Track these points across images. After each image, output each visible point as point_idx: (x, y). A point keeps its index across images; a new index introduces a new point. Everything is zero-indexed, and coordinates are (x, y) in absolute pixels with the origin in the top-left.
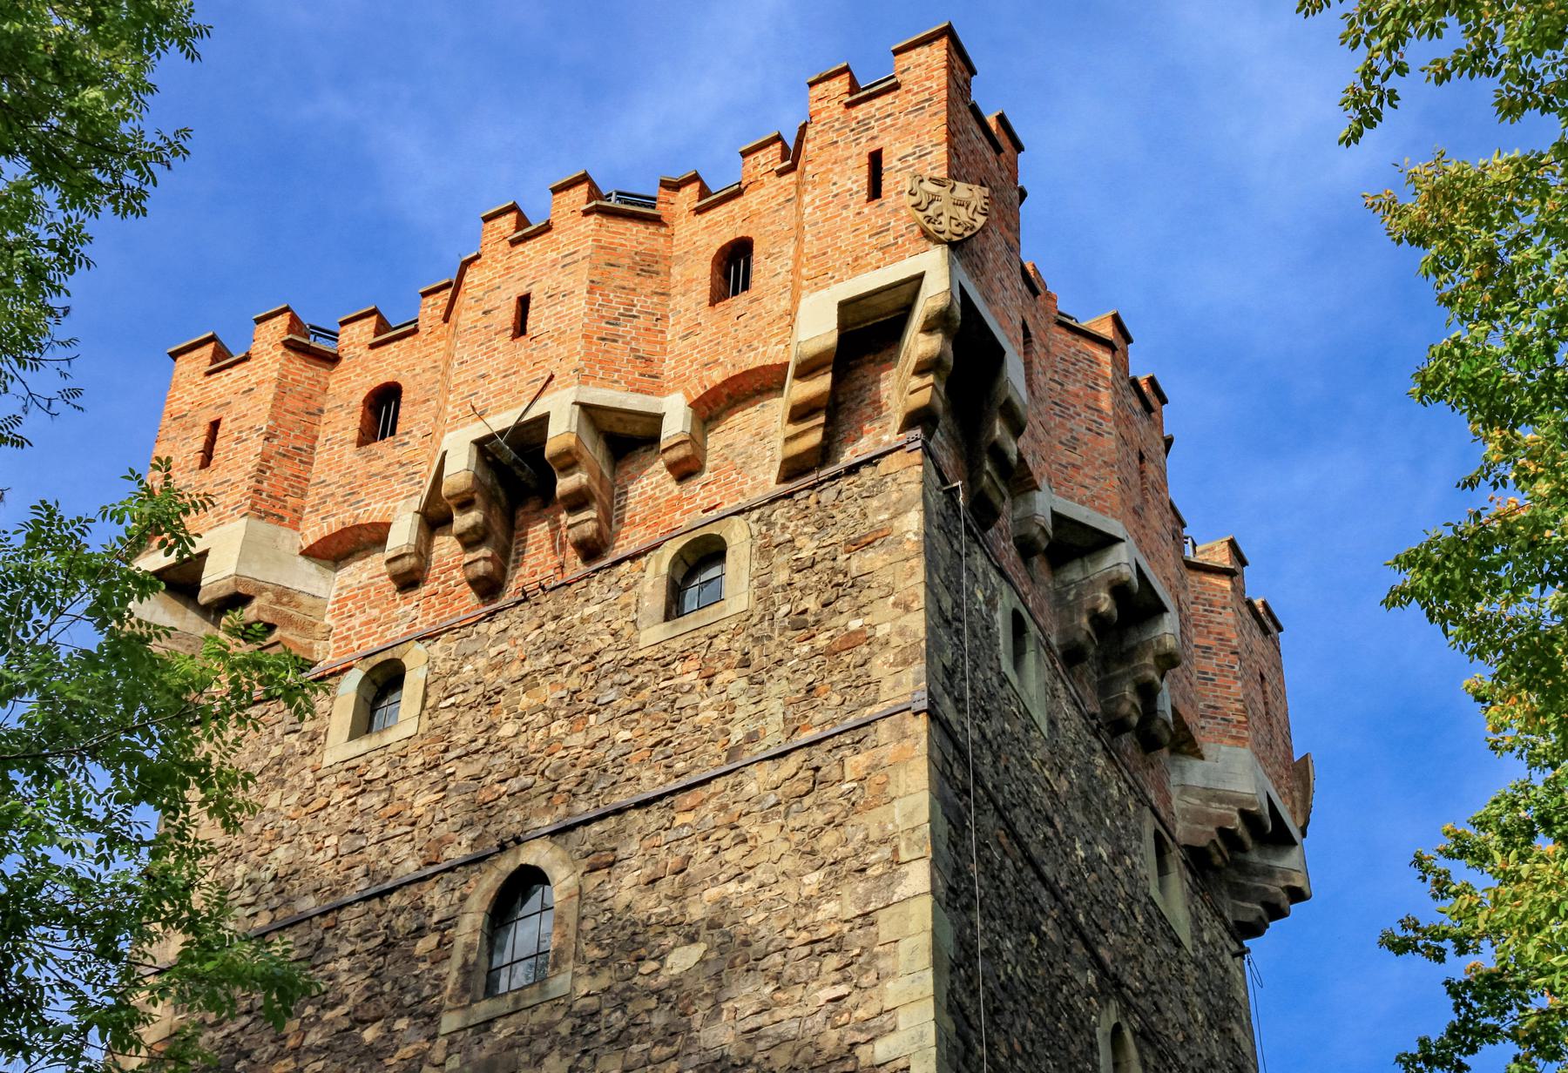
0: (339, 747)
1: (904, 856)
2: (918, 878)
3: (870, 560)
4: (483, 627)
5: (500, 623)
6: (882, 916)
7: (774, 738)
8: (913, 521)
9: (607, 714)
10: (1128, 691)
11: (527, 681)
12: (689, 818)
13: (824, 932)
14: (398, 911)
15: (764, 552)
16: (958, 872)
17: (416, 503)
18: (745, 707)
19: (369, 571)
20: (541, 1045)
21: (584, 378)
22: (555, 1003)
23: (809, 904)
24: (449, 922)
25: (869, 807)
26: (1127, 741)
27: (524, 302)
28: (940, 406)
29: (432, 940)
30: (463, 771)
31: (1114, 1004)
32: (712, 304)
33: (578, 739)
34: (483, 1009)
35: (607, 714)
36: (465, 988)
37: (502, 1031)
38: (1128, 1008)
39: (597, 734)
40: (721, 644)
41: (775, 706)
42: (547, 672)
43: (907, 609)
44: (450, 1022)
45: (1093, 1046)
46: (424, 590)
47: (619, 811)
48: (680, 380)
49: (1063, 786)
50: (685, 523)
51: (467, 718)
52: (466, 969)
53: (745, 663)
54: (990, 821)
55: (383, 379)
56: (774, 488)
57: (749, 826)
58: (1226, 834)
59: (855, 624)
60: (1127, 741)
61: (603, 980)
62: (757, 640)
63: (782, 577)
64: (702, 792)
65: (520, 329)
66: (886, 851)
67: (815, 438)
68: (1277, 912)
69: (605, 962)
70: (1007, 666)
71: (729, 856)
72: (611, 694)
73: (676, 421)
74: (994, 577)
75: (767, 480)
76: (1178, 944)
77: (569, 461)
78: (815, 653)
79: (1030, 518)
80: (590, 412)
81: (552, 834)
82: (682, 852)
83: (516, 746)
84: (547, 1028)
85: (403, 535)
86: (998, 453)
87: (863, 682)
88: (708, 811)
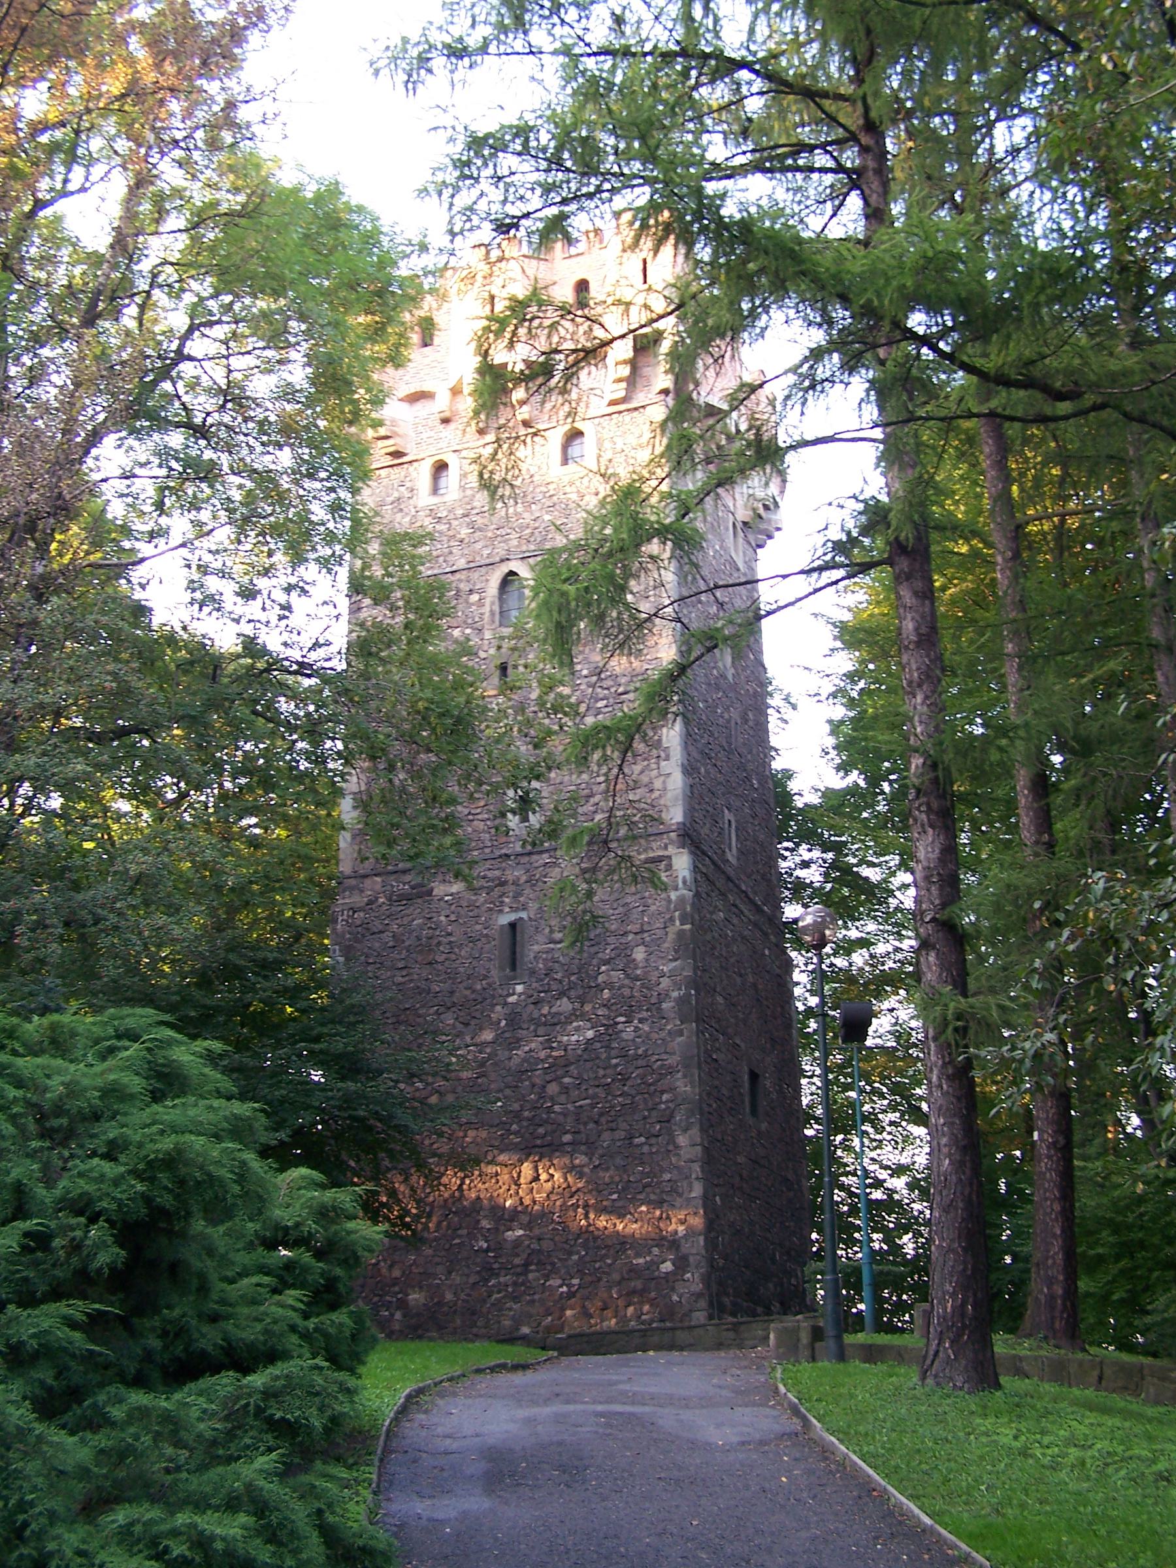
14: (460, 580)
52: (492, 613)
67: (622, 394)
68: (770, 537)
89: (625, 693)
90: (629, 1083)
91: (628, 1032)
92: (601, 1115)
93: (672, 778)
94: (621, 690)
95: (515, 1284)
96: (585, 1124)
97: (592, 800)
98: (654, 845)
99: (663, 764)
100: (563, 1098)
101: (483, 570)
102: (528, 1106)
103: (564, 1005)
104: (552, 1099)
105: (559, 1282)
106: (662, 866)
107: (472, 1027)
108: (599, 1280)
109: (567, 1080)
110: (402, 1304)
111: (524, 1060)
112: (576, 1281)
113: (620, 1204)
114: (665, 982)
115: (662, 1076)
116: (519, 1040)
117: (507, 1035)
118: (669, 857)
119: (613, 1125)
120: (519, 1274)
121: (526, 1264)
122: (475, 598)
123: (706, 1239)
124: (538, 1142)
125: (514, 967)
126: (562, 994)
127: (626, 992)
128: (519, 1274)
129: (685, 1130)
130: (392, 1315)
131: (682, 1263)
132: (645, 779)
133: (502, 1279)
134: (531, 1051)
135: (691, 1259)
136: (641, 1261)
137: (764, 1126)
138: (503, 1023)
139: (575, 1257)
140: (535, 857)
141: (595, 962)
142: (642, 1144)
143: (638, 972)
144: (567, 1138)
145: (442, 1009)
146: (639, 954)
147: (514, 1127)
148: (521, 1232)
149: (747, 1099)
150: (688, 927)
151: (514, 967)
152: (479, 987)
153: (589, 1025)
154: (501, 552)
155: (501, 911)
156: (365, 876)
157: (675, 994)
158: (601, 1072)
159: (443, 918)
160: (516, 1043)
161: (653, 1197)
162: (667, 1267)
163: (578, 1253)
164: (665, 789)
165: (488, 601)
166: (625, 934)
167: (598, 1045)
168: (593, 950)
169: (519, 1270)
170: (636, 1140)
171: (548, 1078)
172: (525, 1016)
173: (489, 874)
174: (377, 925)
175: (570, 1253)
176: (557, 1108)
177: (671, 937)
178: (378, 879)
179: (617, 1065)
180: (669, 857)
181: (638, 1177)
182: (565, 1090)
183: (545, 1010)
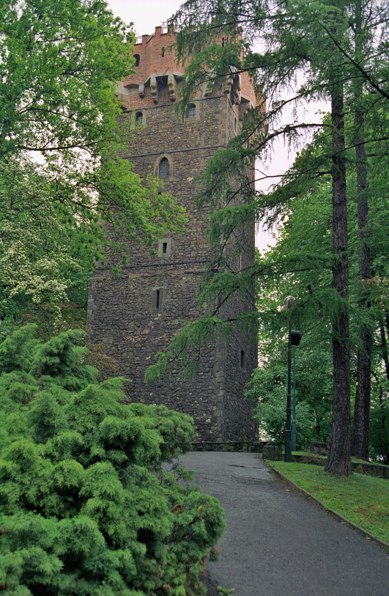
9: (176, 133)
15: (201, 109)
18: (198, 138)
19: (134, 92)
35: (176, 133)
39: (175, 136)
53: (199, 130)
61: (178, 179)
63: (205, 115)
64: (192, 152)
77: (171, 85)
97: (191, 246)
101: (154, 156)
103: (176, 322)
107: (141, 328)
111: (159, 342)
113: (193, 396)
115: (211, 351)
122: (150, 166)
125: (158, 307)
131: (214, 420)
137: (245, 371)
140: (168, 266)
142: (202, 375)
149: (240, 361)
151: (158, 307)
154: (161, 149)
162: (209, 421)
170: (200, 374)
173: (150, 271)
174: (107, 288)
183: (169, 324)
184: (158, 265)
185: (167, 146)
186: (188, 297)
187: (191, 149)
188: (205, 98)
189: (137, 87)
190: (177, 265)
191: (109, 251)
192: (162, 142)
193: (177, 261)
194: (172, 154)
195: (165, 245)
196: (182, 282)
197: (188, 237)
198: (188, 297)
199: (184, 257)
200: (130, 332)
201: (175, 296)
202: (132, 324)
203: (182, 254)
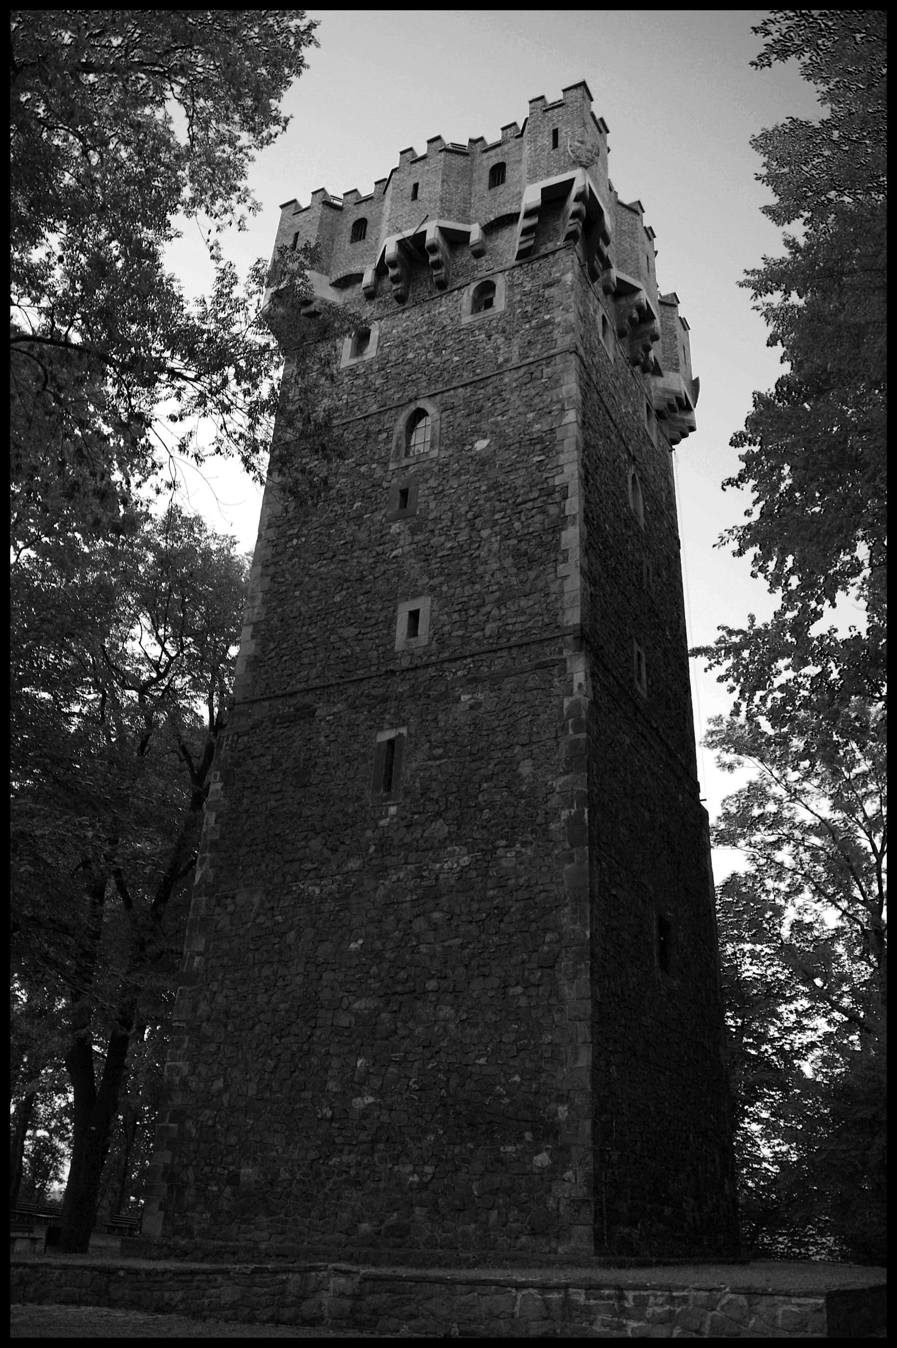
0: (346, 360)
1: (566, 407)
2: (572, 416)
3: (553, 291)
4: (400, 315)
5: (407, 314)
6: (558, 430)
7: (515, 361)
8: (569, 277)
9: (449, 350)
10: (640, 349)
11: (418, 337)
12: (482, 391)
13: (535, 436)
15: (511, 287)
16: (584, 415)
17: (374, 266)
19: (355, 293)
20: (428, 476)
21: (441, 217)
22: (432, 460)
23: (530, 425)
24: (392, 429)
25: (552, 388)
26: (637, 369)
27: (416, 186)
28: (580, 231)
29: (385, 435)
30: (394, 371)
31: (633, 467)
32: (490, 188)
33: (437, 360)
34: (405, 462)
35: (449, 350)
36: (398, 454)
37: (412, 470)
38: (637, 468)
40: (494, 324)
41: (516, 348)
42: (425, 333)
43: (568, 311)
44: (392, 466)
45: (626, 481)
46: (377, 300)
47: (455, 388)
48: (477, 219)
49: (618, 385)
50: (479, 276)
51: (394, 351)
52: (398, 447)
53: (504, 331)
54: (595, 396)
55: (360, 217)
56: (514, 262)
57: (506, 395)
58: (670, 406)
59: (547, 317)
60: (637, 369)
61: (450, 452)
62: (508, 322)
63: (518, 297)
65: (415, 196)
66: (559, 406)
67: (531, 243)
68: (685, 436)
69: (451, 445)
70: (601, 337)
71: (498, 406)
72: (451, 343)
73: (475, 232)
74: (596, 302)
75: (511, 259)
76: (653, 446)
77: (434, 249)
78: (531, 328)
79: (609, 279)
80: (443, 231)
81: (429, 396)
82: (480, 404)
83: (415, 362)
84: (429, 470)
85: (368, 278)
86: (600, 253)
87: (550, 341)
88: (490, 389)
89: (525, 502)
90: (506, 919)
91: (508, 859)
92: (473, 956)
93: (569, 580)
94: (520, 500)
95: (359, 1164)
96: (453, 969)
97: (488, 608)
98: (547, 650)
99: (560, 567)
100: (431, 936)
101: (393, 412)
102: (390, 945)
103: (440, 829)
104: (417, 936)
105: (410, 1168)
106: (555, 671)
108: (457, 1169)
109: (436, 915)
110: (234, 1179)
112: (429, 1169)
114: (555, 800)
116: (386, 869)
117: (374, 862)
118: (565, 660)
119: (486, 970)
120: (364, 1153)
121: (374, 1142)
123: (594, 1124)
124: (399, 988)
125: (388, 786)
126: (438, 815)
127: (509, 811)
128: (364, 1153)
129: (571, 980)
130: (221, 1191)
132: (540, 584)
133: (345, 1158)
134: (399, 880)
135: (573, 1150)
136: (510, 1149)
138: (372, 849)
139: (431, 1137)
140: (421, 672)
141: (476, 779)
143: (524, 788)
144: (432, 985)
145: (311, 834)
146: (526, 769)
147: (374, 969)
148: (371, 1100)
150: (583, 735)
151: (388, 786)
152: (350, 810)
153: (465, 850)
154: (411, 392)
155: (381, 729)
156: (254, 702)
157: (565, 814)
158: (475, 906)
159: (322, 739)
160: (382, 871)
161: (529, 1065)
163: (434, 1131)
164: (562, 592)
165: (395, 437)
166: (511, 746)
167: (473, 874)
168: (473, 765)
169: (364, 1147)
170: (512, 991)
171: (415, 912)
172: (396, 842)
173: (374, 692)
175: (426, 1131)
176: (423, 948)
177: (564, 747)
178: (266, 704)
179: (493, 898)
180: (565, 660)
181: (513, 1037)
182: (434, 927)
184: (393, 672)
185: (425, 384)
186: (475, 750)
187: (484, 375)
188: (517, 262)
189: (359, 277)
190: (446, 665)
191: (273, 654)
192: (414, 377)
193: (446, 655)
194: (438, 397)
195: (414, 616)
196: (461, 707)
197: (477, 587)
198: (475, 750)
199: (465, 640)
200: (310, 866)
201: (440, 751)
202: (316, 844)
203: (461, 633)
